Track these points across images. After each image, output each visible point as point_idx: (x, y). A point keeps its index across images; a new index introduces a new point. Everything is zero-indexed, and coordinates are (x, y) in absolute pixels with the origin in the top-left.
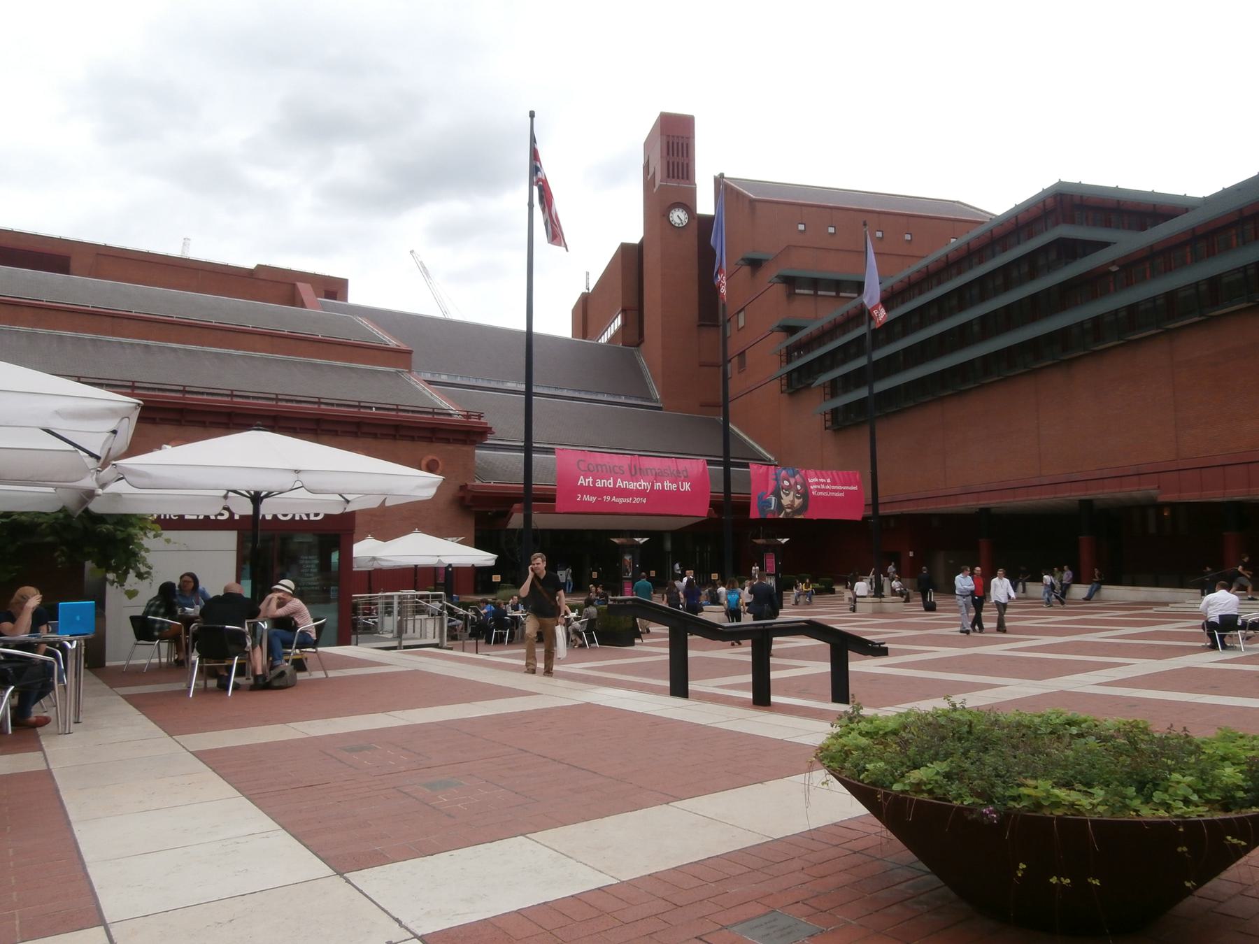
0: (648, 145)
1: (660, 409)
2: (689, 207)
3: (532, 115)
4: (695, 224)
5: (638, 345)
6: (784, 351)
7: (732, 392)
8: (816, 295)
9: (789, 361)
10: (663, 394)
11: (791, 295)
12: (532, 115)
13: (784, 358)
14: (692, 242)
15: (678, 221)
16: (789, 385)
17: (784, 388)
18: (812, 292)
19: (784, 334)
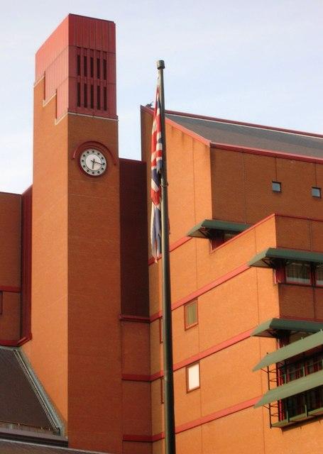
0: (41, 55)
1: (64, 444)
2: (108, 147)
3: (162, 67)
4: (115, 171)
5: (19, 345)
6: (273, 367)
7: (178, 423)
8: (314, 286)
9: (281, 380)
10: (73, 422)
11: (283, 286)
12: (162, 67)
13: (273, 376)
14: (111, 196)
15: (97, 167)
16: (282, 415)
17: (275, 420)
18: (308, 282)
19: (272, 341)
